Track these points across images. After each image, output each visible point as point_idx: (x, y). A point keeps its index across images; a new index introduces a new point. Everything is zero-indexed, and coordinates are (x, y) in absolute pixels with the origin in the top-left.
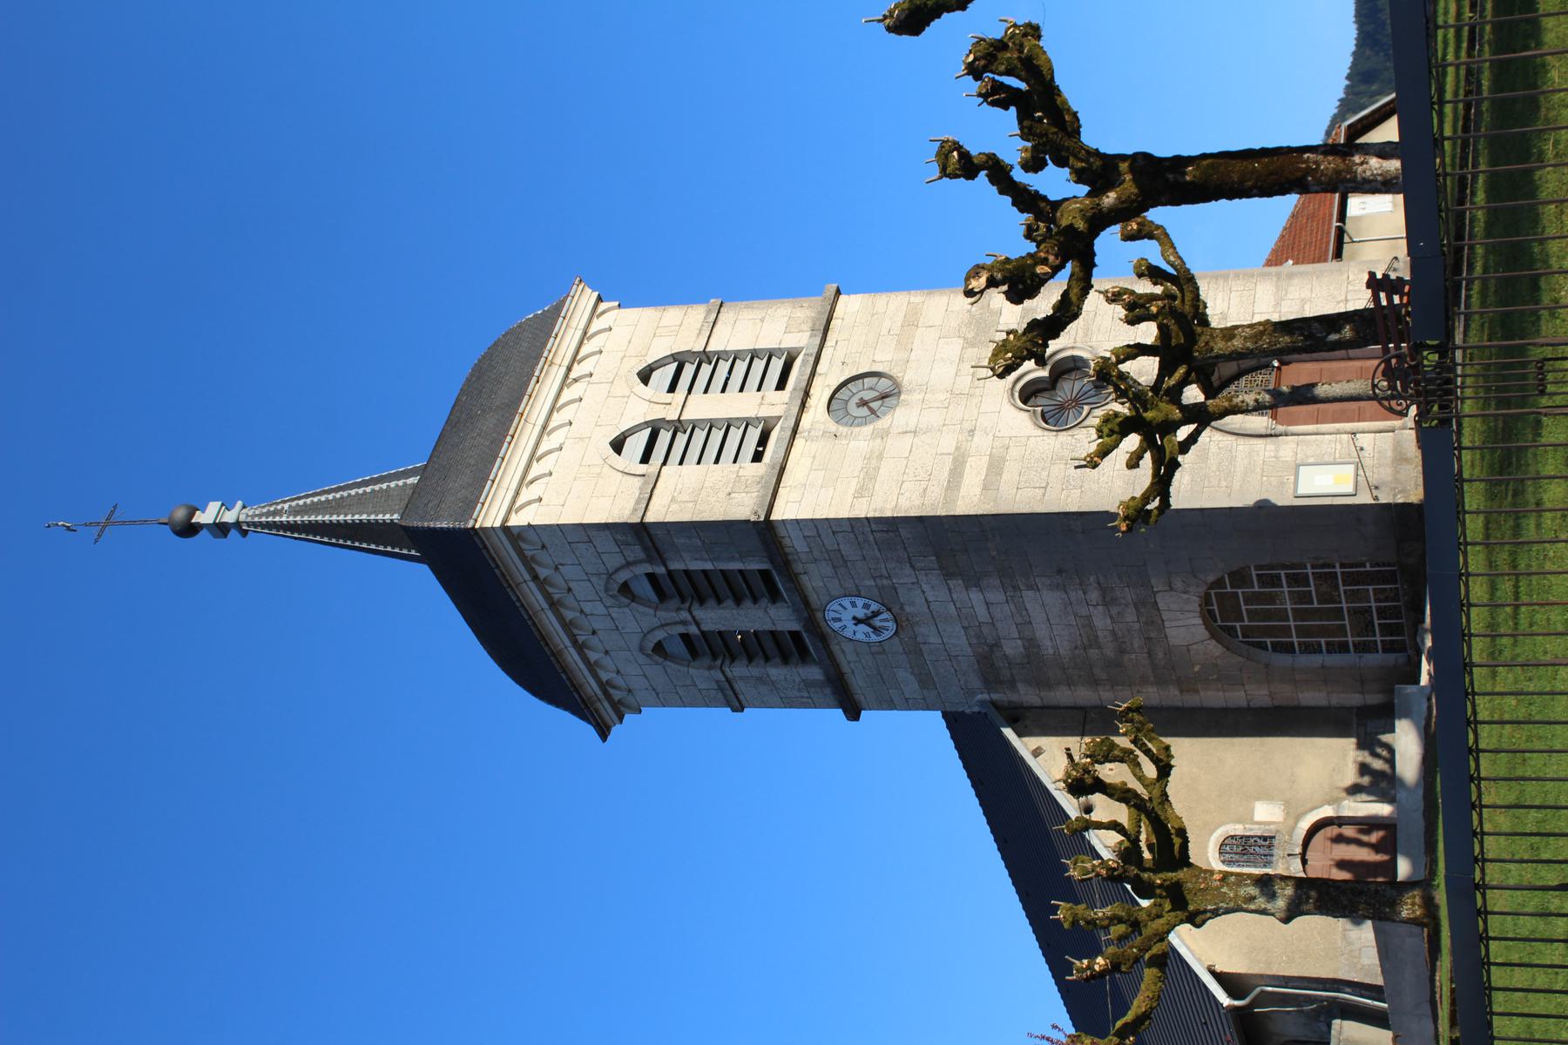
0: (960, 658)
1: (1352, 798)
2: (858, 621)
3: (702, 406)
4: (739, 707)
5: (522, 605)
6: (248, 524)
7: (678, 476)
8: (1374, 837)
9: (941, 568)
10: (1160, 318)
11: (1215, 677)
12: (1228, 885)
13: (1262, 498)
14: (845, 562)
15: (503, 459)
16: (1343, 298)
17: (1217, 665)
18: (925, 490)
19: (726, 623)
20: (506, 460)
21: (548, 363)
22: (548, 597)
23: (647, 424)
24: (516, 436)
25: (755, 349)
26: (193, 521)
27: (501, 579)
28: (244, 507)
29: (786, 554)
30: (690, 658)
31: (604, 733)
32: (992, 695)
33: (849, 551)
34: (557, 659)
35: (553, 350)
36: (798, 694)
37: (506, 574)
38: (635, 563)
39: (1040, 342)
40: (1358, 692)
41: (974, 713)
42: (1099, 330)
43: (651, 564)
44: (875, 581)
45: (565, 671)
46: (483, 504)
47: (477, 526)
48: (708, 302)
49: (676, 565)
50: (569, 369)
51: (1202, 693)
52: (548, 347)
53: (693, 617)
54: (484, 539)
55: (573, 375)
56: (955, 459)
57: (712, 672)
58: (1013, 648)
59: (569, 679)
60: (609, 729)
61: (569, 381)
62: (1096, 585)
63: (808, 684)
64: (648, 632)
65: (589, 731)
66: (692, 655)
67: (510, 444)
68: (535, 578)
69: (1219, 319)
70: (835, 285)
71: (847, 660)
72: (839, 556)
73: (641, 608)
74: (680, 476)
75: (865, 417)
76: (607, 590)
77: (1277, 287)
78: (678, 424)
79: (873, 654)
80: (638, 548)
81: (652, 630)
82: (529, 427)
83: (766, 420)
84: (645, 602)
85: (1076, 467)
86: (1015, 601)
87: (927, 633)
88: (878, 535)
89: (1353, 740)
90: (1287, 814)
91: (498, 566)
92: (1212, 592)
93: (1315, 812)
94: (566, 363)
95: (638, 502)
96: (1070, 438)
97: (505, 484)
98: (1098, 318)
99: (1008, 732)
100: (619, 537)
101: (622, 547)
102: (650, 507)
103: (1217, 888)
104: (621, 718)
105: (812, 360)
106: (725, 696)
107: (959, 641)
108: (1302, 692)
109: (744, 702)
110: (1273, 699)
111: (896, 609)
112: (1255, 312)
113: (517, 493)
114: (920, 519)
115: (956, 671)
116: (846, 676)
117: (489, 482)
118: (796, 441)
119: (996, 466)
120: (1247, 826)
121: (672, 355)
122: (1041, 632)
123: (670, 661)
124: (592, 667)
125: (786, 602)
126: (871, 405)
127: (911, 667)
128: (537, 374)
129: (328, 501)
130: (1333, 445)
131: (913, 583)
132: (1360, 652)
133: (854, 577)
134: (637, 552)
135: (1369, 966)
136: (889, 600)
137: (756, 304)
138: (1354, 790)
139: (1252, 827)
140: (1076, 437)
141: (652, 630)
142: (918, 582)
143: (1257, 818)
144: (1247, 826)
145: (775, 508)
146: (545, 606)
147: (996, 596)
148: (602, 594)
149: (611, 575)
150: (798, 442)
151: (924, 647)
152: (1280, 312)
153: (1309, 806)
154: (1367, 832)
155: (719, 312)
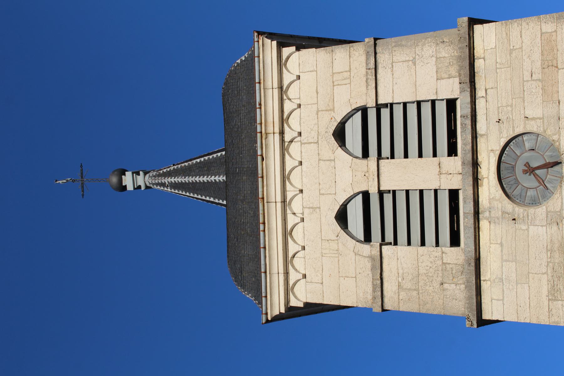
7: (396, 258)
15: (265, 248)
24: (266, 222)
35: (263, 121)
46: (266, 297)
48: (364, 41)
50: (282, 133)
52: (258, 121)
61: (286, 144)
67: (264, 231)
74: (398, 259)
75: (536, 188)
94: (277, 130)
97: (275, 270)
102: (385, 293)
105: (468, 122)
117: (263, 275)
118: (481, 223)
126: (538, 172)
128: (259, 153)
137: (403, 40)
150: (484, 224)
155: (376, 53)
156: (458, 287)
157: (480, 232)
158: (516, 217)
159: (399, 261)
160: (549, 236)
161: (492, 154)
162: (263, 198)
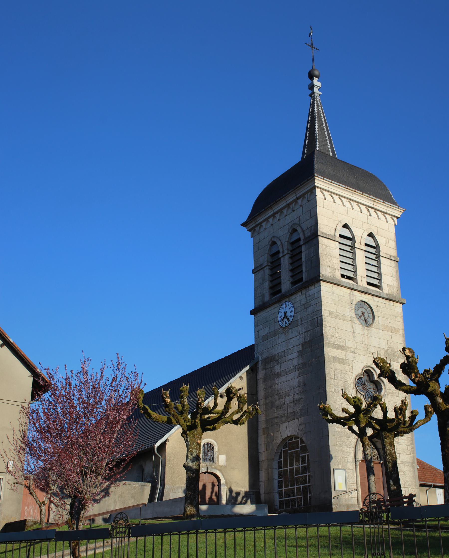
0: (273, 350)
1: (227, 490)
2: (285, 313)
3: (360, 256)
4: (254, 272)
5: (288, 194)
6: (314, 97)
7: (335, 248)
8: (214, 498)
9: (305, 342)
10: (397, 419)
11: (269, 441)
12: (196, 445)
13: (333, 457)
14: (306, 308)
15: (339, 185)
16: (406, 486)
17: (273, 441)
18: (333, 336)
19: (284, 266)
20: (339, 187)
21: (374, 200)
22: (291, 203)
23: (353, 236)
25: (381, 274)
26: (314, 77)
27: (297, 187)
28: (320, 95)
29: (308, 287)
30: (271, 254)
31: (244, 225)
32: (261, 361)
33: (310, 310)
34: (269, 207)
36: (259, 293)
37: (299, 188)
38: (304, 234)
39: (387, 375)
40: (265, 492)
41: (254, 355)
42: (392, 398)
43: (304, 239)
44: (300, 319)
45: (265, 210)
46: (323, 179)
47: (315, 177)
49: (303, 248)
50: (372, 208)
51: (263, 436)
52: (380, 200)
53: (285, 255)
54: (311, 180)
55: (370, 209)
56: (344, 347)
57: (266, 262)
58: (277, 368)
59: (262, 212)
60: (245, 226)
62: (300, 398)
63: (263, 296)
64: (279, 239)
65: (244, 219)
66: (272, 255)
67: (345, 188)
68: (298, 199)
69: (397, 441)
70: (405, 302)
71: (272, 310)
72: (308, 306)
73: (288, 237)
75: (358, 314)
76: (294, 224)
77: (409, 462)
78: (354, 247)
79: (274, 319)
80: (309, 234)
81: (280, 241)
82: (351, 195)
83: (356, 279)
84: (290, 238)
85: (342, 389)
86: (294, 369)
87: (282, 338)
88: (316, 320)
89: (248, 490)
90: (222, 467)
91: (301, 185)
92: (299, 439)
93: (223, 476)
94: (375, 207)
95: (326, 234)
96: (353, 388)
97: (330, 186)
98: (396, 398)
99: (248, 367)
100: (313, 228)
101: (309, 229)
102: (324, 238)
103: (195, 442)
104: (249, 230)
105: (378, 295)
106: (258, 267)
107: (279, 350)
108: (264, 472)
109: (256, 274)
110: (262, 461)
111: (290, 327)
113: (327, 191)
114: (322, 335)
115: (269, 348)
116: (266, 310)
117: (331, 181)
118: (349, 290)
119: (342, 361)
120: (217, 452)
121: (378, 244)
122: (283, 379)
123: (270, 247)
124: (267, 220)
125: (291, 287)
126: (363, 316)
127: (270, 332)
128: (370, 196)
129: (323, 124)
130: (352, 483)
131: (299, 332)
132: (279, 492)
133: (301, 312)
134: (308, 234)
135: (170, 496)
136: (293, 324)
137: (398, 274)
138: (231, 490)
139: (217, 454)
140: (353, 390)
141: (280, 241)
142: (300, 334)
143: (220, 456)
144: (217, 452)
145: (325, 283)
146: (288, 202)
147: (296, 362)
148: (292, 223)
149: (299, 225)
150: (349, 291)
151: (277, 337)
153: (225, 475)
154: (216, 495)
155: (394, 261)
156: (329, 273)
157: (346, 288)
158: (351, 305)
159: (334, 249)
160: (347, 316)
161: (368, 300)
162: (356, 192)
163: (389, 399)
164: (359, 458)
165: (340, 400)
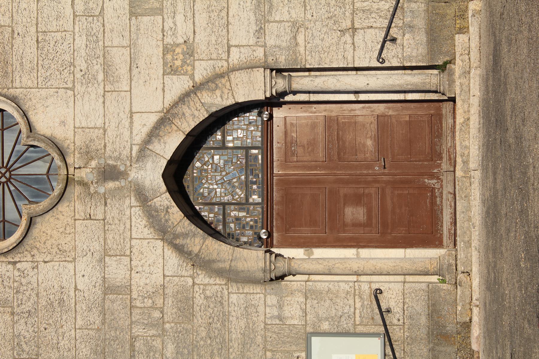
16: (349, 24)
42: (21, 64)
69: (183, 53)
96: (10, 267)
98: (18, 41)
112: (232, 43)
130: (351, 302)
140: (18, 265)
152: (265, 46)
163: (30, 84)
164: (261, 264)
165: (64, 334)
